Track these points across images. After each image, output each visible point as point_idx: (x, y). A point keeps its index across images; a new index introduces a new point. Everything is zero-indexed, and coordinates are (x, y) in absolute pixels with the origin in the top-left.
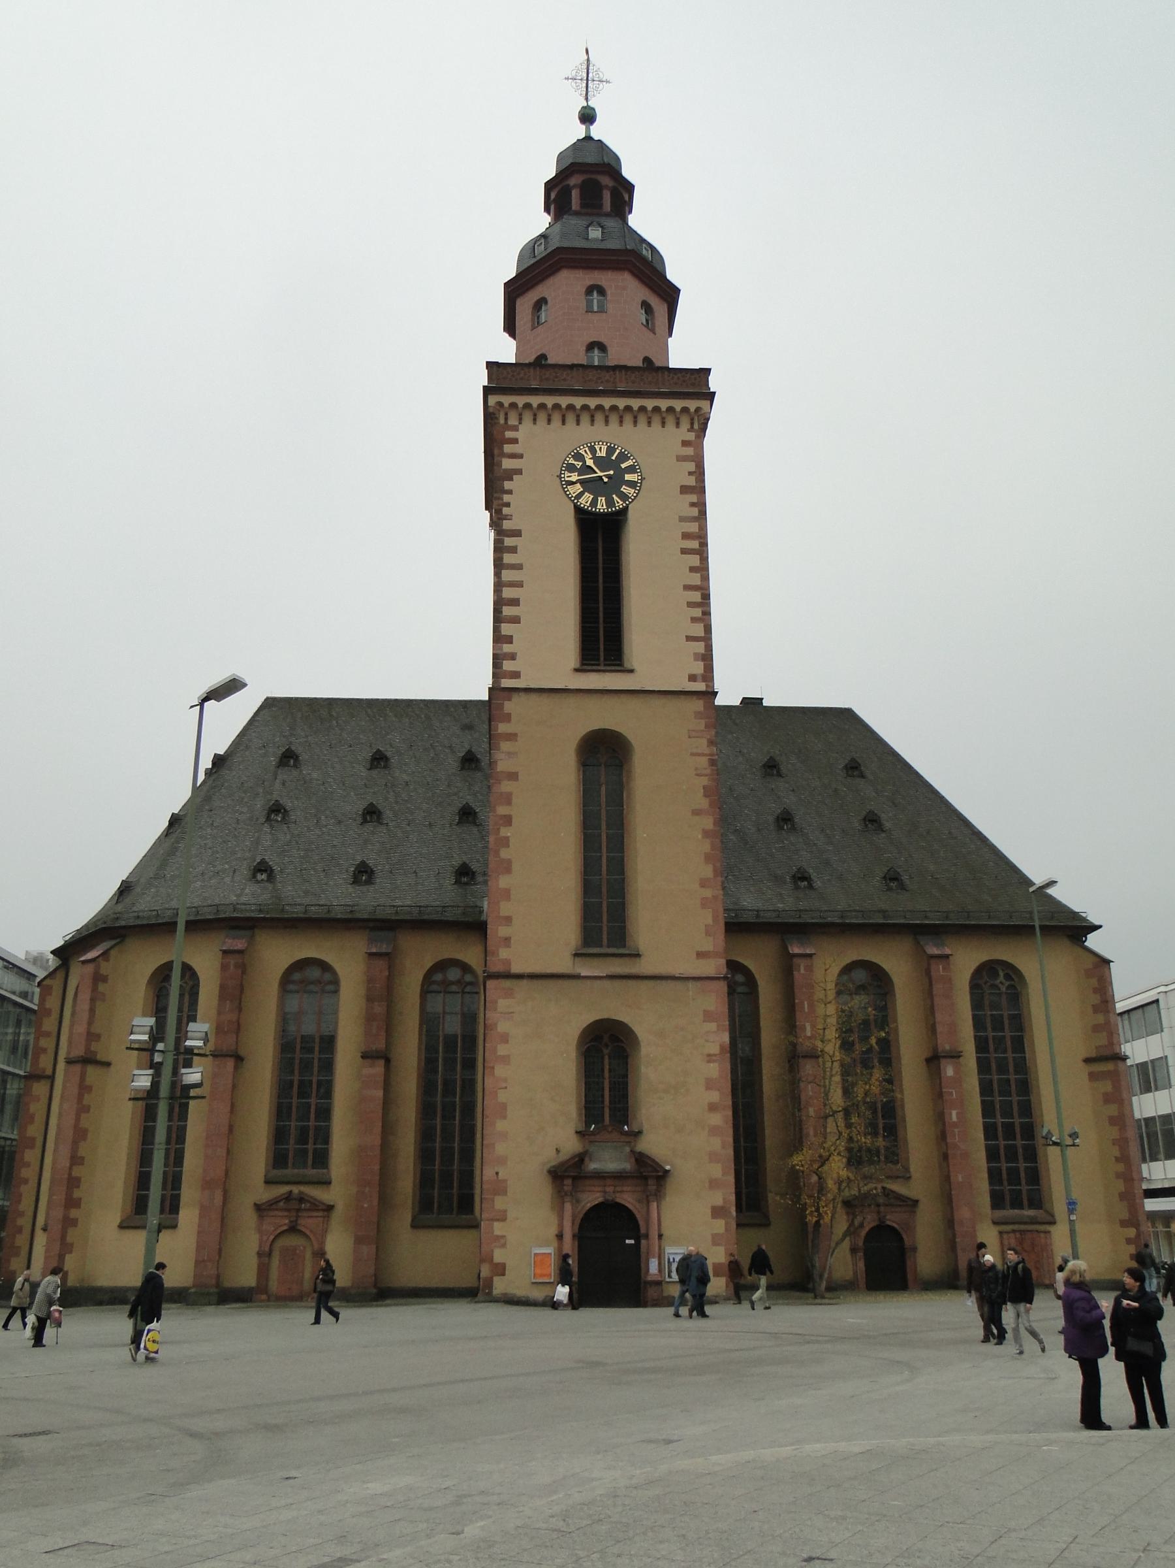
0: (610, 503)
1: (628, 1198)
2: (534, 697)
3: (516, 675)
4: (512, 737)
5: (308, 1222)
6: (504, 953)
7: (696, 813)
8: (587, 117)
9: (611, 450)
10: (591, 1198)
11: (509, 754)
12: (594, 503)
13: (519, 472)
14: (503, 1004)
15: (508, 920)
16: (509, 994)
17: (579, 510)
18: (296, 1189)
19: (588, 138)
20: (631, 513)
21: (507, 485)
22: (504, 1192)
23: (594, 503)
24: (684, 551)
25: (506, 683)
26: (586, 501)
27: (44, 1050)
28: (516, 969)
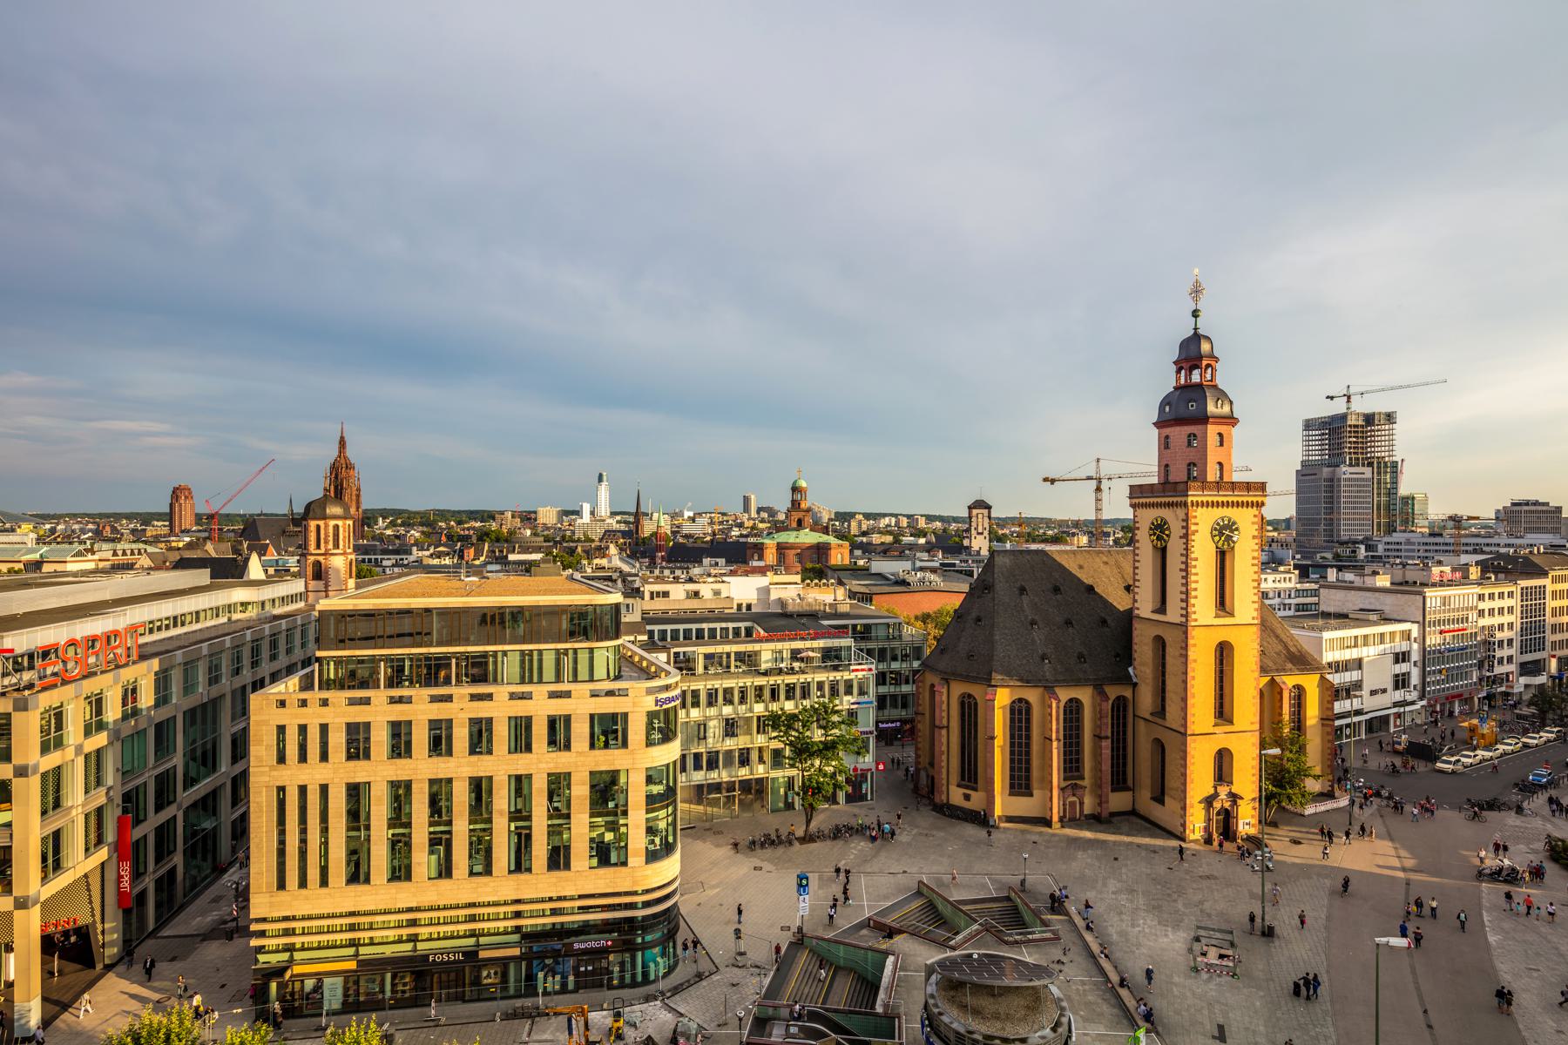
0: (1229, 545)
3: (1196, 620)
5: (1079, 792)
8: (1195, 314)
9: (1229, 521)
13: (1197, 531)
15: (1194, 715)
16: (1195, 741)
19: (1196, 329)
24: (1253, 565)
25: (1193, 624)
26: (1220, 545)
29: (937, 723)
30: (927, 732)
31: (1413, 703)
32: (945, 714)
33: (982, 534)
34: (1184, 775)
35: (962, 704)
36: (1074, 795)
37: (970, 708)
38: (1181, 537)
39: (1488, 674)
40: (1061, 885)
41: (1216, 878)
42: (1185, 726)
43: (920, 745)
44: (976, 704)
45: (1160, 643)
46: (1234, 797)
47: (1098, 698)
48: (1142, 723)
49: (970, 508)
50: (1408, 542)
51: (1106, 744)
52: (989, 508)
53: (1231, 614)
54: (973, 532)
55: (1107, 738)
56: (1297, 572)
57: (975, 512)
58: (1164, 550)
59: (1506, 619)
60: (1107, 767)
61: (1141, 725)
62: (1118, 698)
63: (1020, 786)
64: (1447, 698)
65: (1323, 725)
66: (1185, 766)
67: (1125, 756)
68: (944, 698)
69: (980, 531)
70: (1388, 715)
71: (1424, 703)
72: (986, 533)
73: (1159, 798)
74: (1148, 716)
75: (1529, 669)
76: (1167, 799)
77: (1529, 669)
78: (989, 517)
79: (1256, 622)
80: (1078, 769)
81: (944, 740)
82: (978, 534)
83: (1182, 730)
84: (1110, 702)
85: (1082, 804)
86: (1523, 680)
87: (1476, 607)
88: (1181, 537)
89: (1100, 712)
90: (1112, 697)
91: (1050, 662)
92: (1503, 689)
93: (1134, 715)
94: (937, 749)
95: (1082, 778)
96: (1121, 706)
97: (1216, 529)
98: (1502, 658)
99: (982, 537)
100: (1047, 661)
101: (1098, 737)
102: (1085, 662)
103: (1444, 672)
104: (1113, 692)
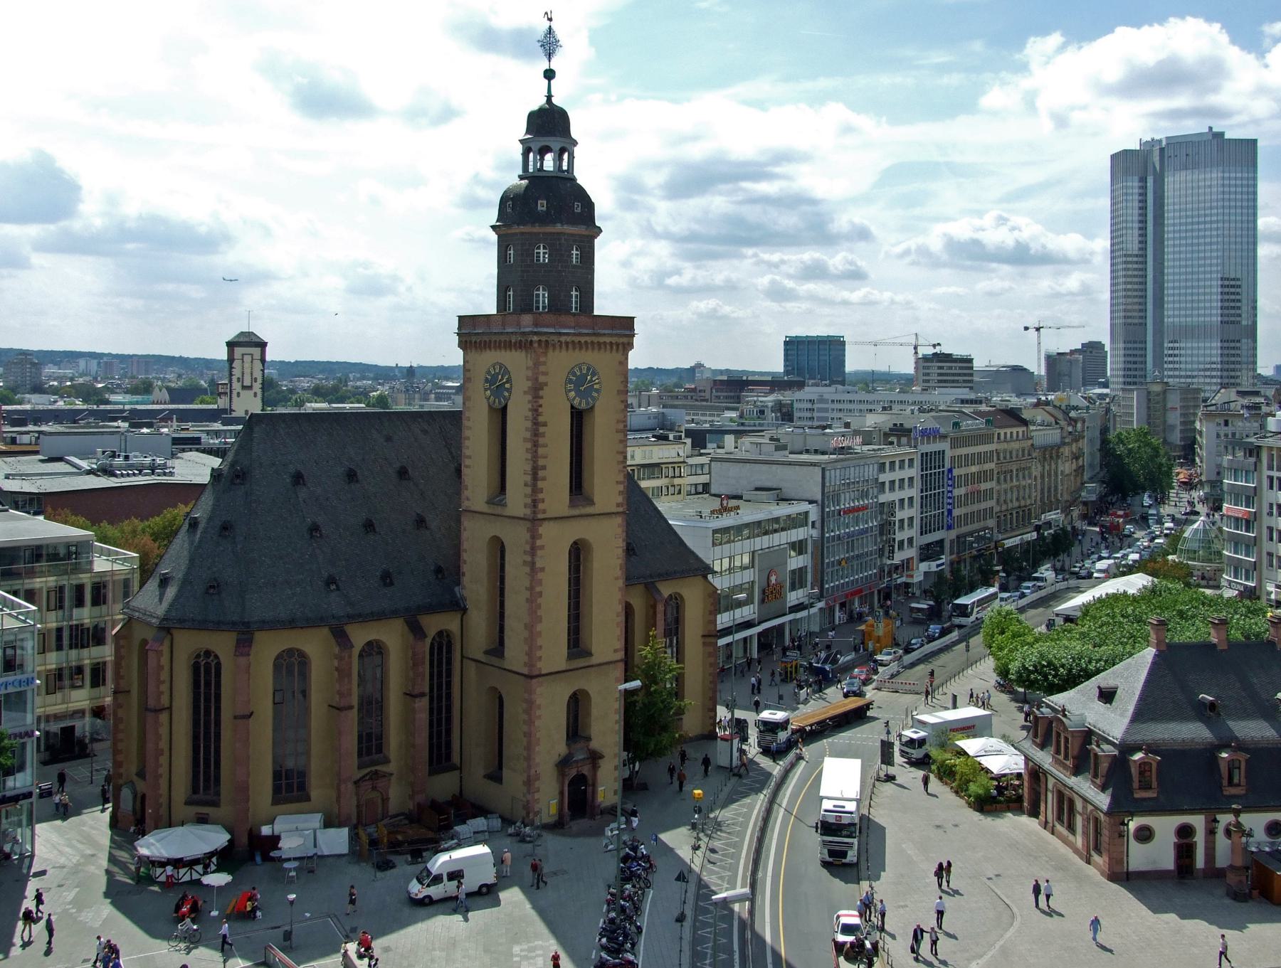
0: (587, 403)
1: (586, 770)
2: (552, 523)
3: (544, 512)
4: (542, 547)
6: (539, 665)
7: (617, 579)
10: (573, 772)
11: (541, 557)
12: (580, 403)
13: (546, 384)
14: (539, 690)
17: (572, 407)
18: (373, 769)
20: (597, 409)
21: (541, 393)
22: (538, 779)
23: (580, 403)
25: (540, 516)
26: (576, 402)
27: (162, 693)
28: (544, 672)
29: (152, 703)
30: (134, 723)
31: (812, 605)
32: (165, 688)
33: (250, 388)
34: (528, 735)
35: (196, 668)
36: (374, 788)
37: (208, 671)
38: (525, 393)
39: (889, 562)
40: (348, 928)
41: (565, 872)
42: (530, 664)
43: (120, 745)
44: (218, 665)
45: (498, 549)
46: (595, 757)
47: (411, 637)
48: (471, 670)
49: (231, 345)
50: (822, 400)
51: (423, 703)
52: (262, 345)
53: (591, 502)
54: (237, 386)
55: (422, 695)
56: (689, 441)
57: (238, 351)
58: (504, 410)
59: (907, 493)
60: (422, 739)
61: (471, 670)
62: (440, 633)
63: (290, 788)
64: (847, 596)
65: (704, 644)
66: (530, 722)
67: (449, 720)
68: (165, 660)
69: (247, 382)
70: (781, 626)
71: (821, 604)
72: (257, 387)
73: (495, 776)
74: (480, 656)
75: (929, 552)
76: (506, 773)
77: (929, 552)
78: (263, 360)
79: (621, 509)
80: (379, 750)
81: (164, 731)
82: (244, 387)
83: (525, 671)
84: (428, 641)
85: (385, 800)
86: (924, 567)
87: (877, 479)
88: (525, 393)
89: (414, 654)
90: (431, 633)
91: (338, 589)
92: (904, 579)
93: (462, 657)
94: (150, 746)
95: (387, 761)
96: (443, 646)
97: (570, 381)
98: (903, 540)
99: (251, 393)
100: (333, 587)
101: (411, 695)
102: (392, 584)
103: (843, 563)
104: (434, 624)
